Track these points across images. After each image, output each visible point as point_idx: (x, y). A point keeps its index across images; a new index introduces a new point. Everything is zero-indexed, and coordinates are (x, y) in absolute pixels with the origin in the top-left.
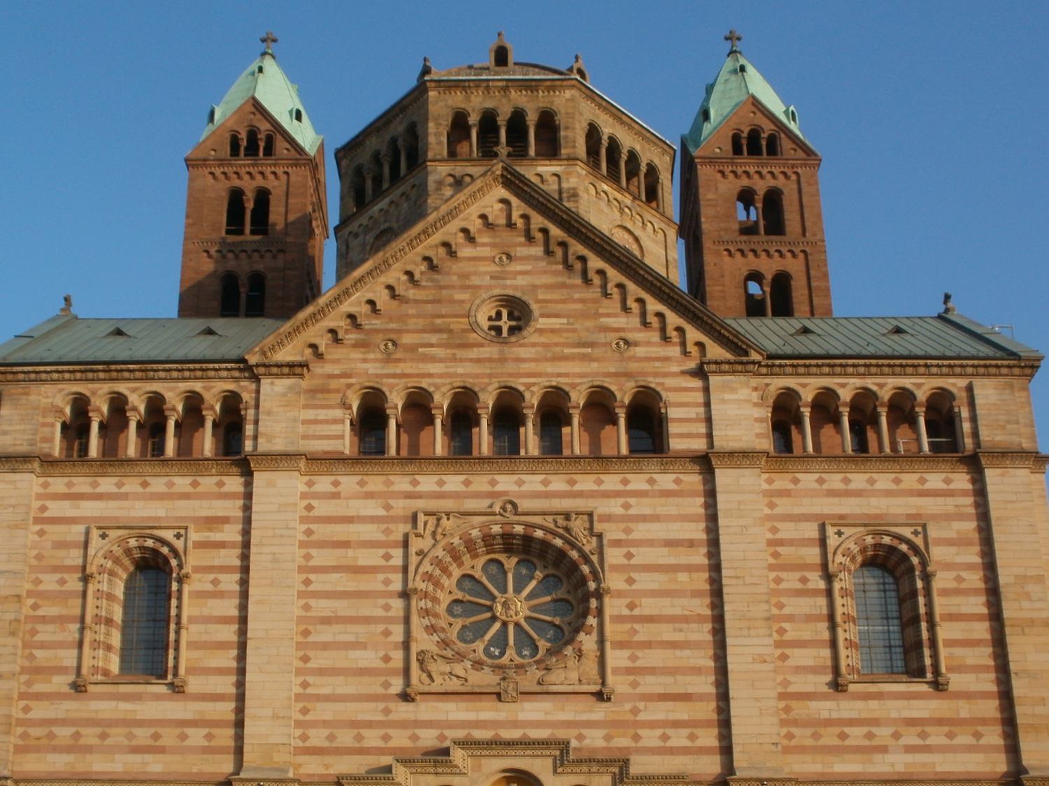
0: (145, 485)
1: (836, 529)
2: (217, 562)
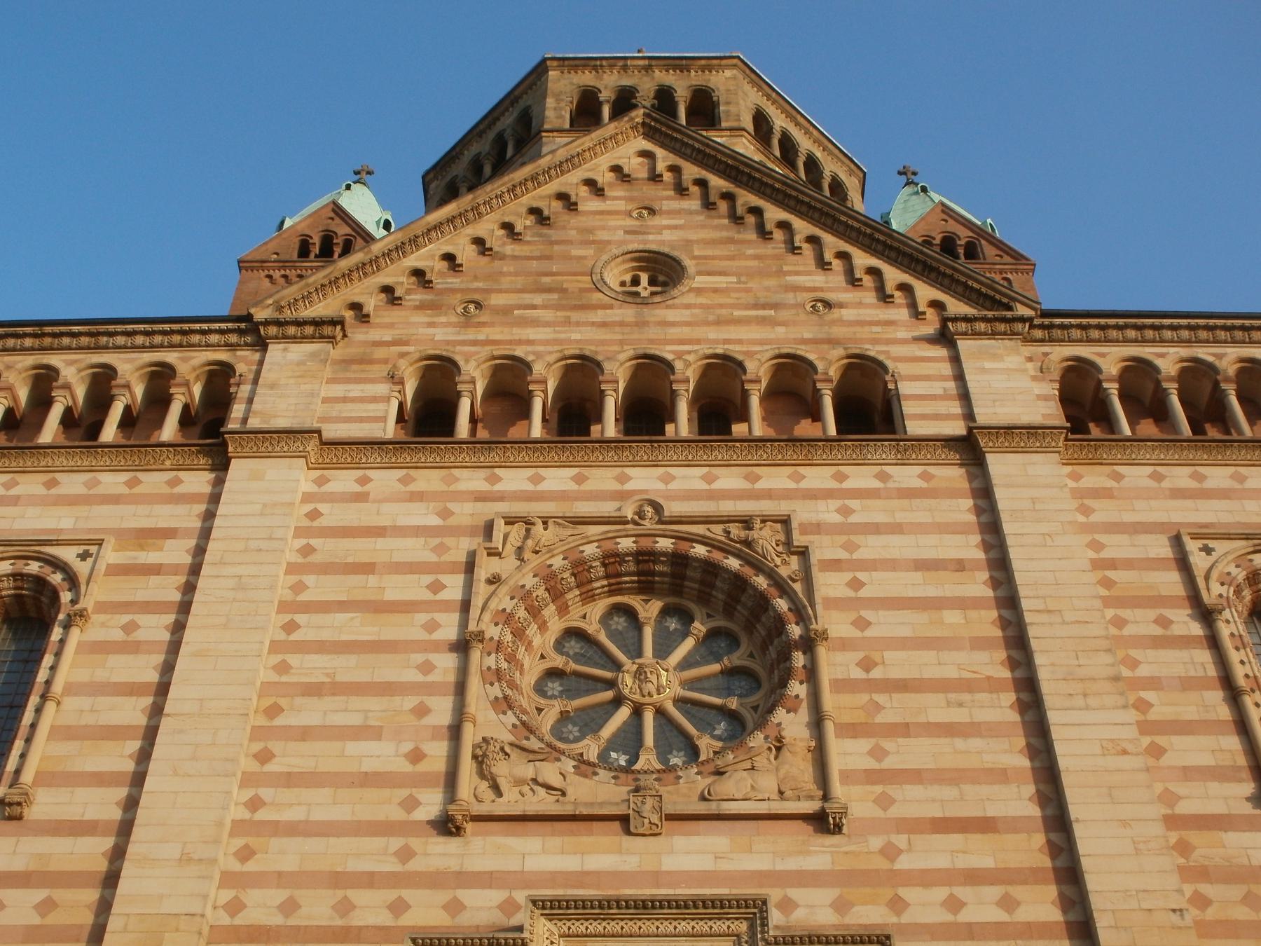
1: (1200, 543)
2: (141, 596)
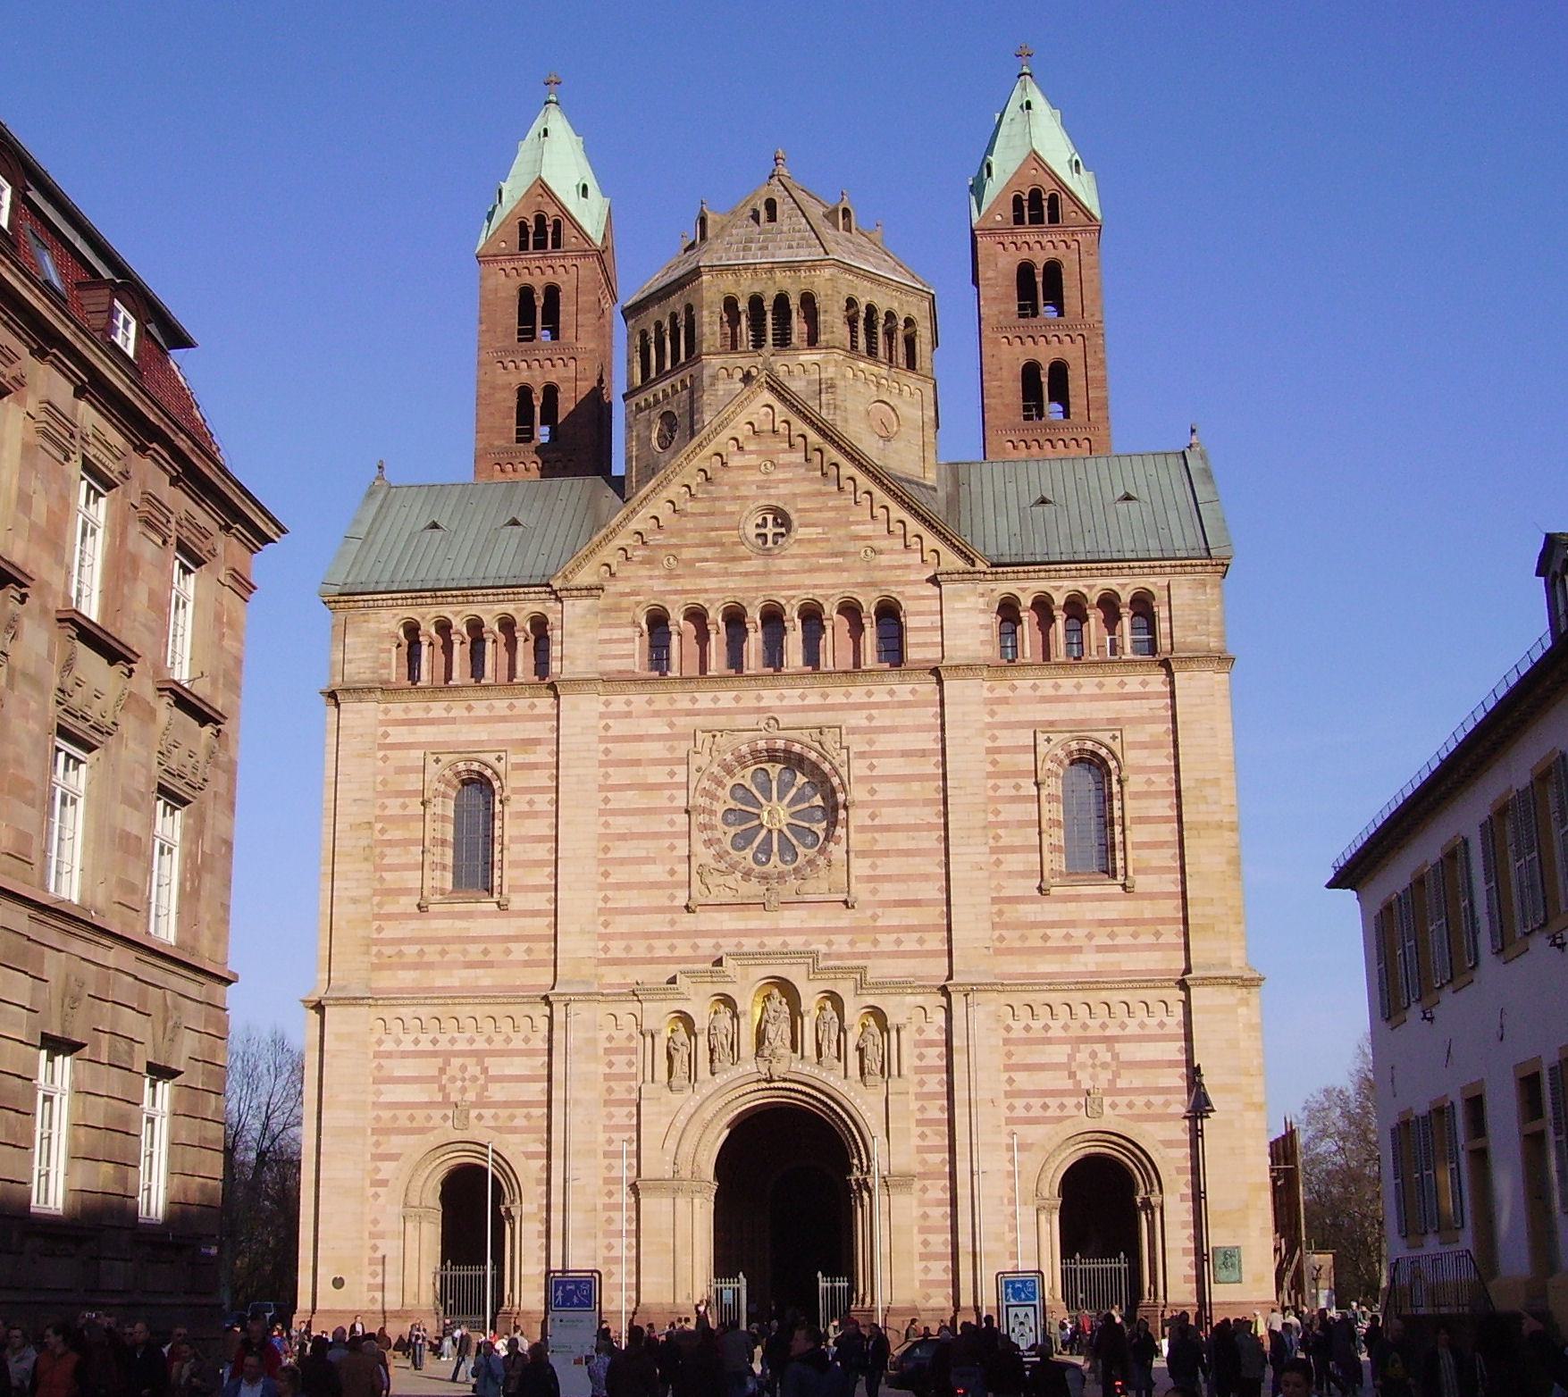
0: (469, 708)
1: (1045, 736)
2: (533, 784)
